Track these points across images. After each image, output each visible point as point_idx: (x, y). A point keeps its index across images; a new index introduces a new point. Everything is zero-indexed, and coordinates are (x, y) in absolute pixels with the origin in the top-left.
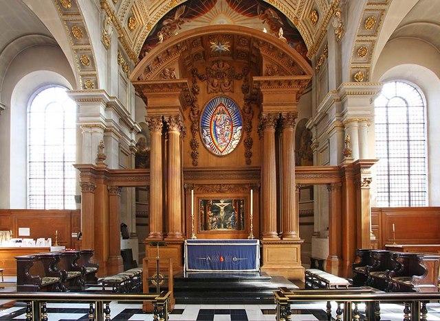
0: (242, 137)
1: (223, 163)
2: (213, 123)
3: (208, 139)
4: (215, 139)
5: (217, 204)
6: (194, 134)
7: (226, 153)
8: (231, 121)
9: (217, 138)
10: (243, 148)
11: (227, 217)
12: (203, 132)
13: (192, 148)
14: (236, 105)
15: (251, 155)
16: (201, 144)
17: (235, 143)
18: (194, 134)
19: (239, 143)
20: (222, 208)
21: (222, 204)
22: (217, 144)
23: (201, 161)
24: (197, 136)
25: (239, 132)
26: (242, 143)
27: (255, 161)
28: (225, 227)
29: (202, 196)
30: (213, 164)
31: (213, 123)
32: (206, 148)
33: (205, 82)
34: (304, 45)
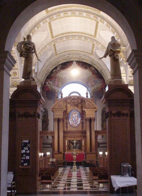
1: (75, 129)
3: (71, 122)
5: (73, 142)
6: (67, 120)
8: (77, 116)
9: (73, 121)
10: (81, 125)
11: (76, 145)
12: (69, 120)
14: (78, 111)
16: (68, 123)
17: (79, 123)
18: (67, 120)
19: (80, 123)
20: (75, 143)
21: (75, 142)
23: (69, 129)
24: (68, 121)
25: (80, 120)
26: (81, 123)
27: (84, 129)
28: (76, 149)
29: (69, 139)
30: (72, 130)
32: (70, 124)
33: (70, 105)
34: (104, 80)
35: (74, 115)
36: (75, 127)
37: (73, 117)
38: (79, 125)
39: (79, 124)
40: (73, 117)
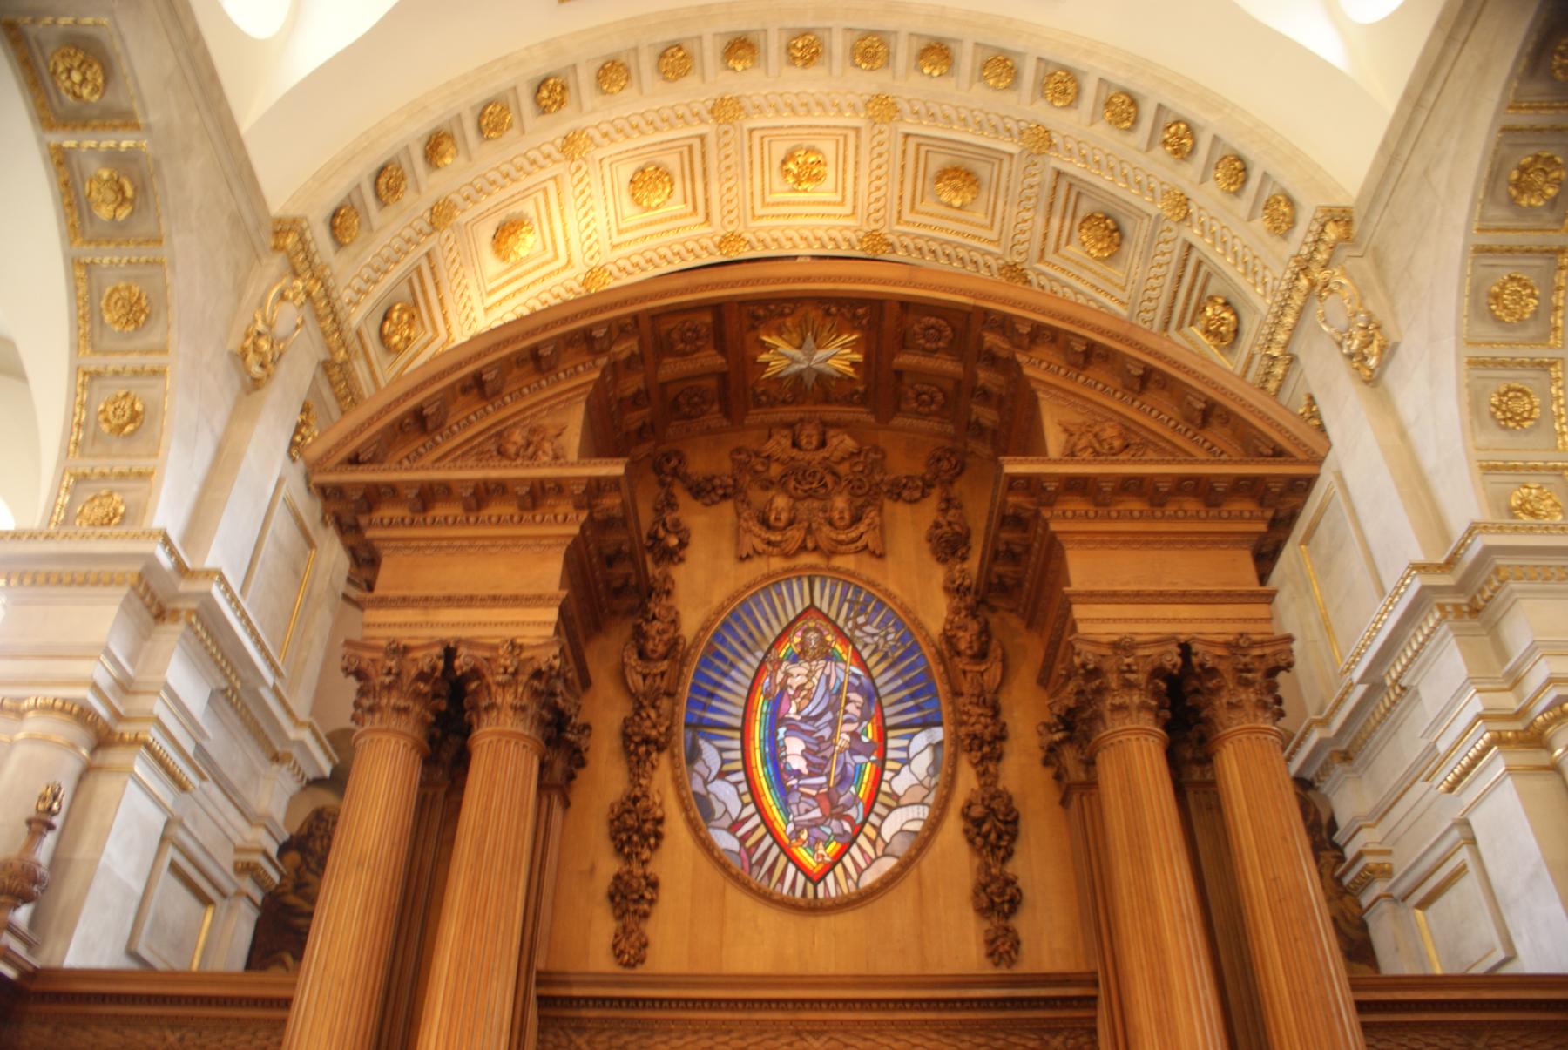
0: (950, 783)
2: (761, 705)
3: (726, 796)
4: (770, 799)
7: (848, 887)
8: (871, 695)
9: (784, 792)
12: (694, 755)
13: (619, 850)
15: (1015, 903)
16: (676, 827)
17: (903, 821)
19: (933, 825)
22: (784, 828)
24: (661, 781)
25: (923, 762)
26: (953, 827)
31: (761, 705)
32: (707, 846)
35: (798, 674)
36: (815, 908)
37: (776, 702)
38: (906, 864)
39: (923, 841)
40: (776, 702)
